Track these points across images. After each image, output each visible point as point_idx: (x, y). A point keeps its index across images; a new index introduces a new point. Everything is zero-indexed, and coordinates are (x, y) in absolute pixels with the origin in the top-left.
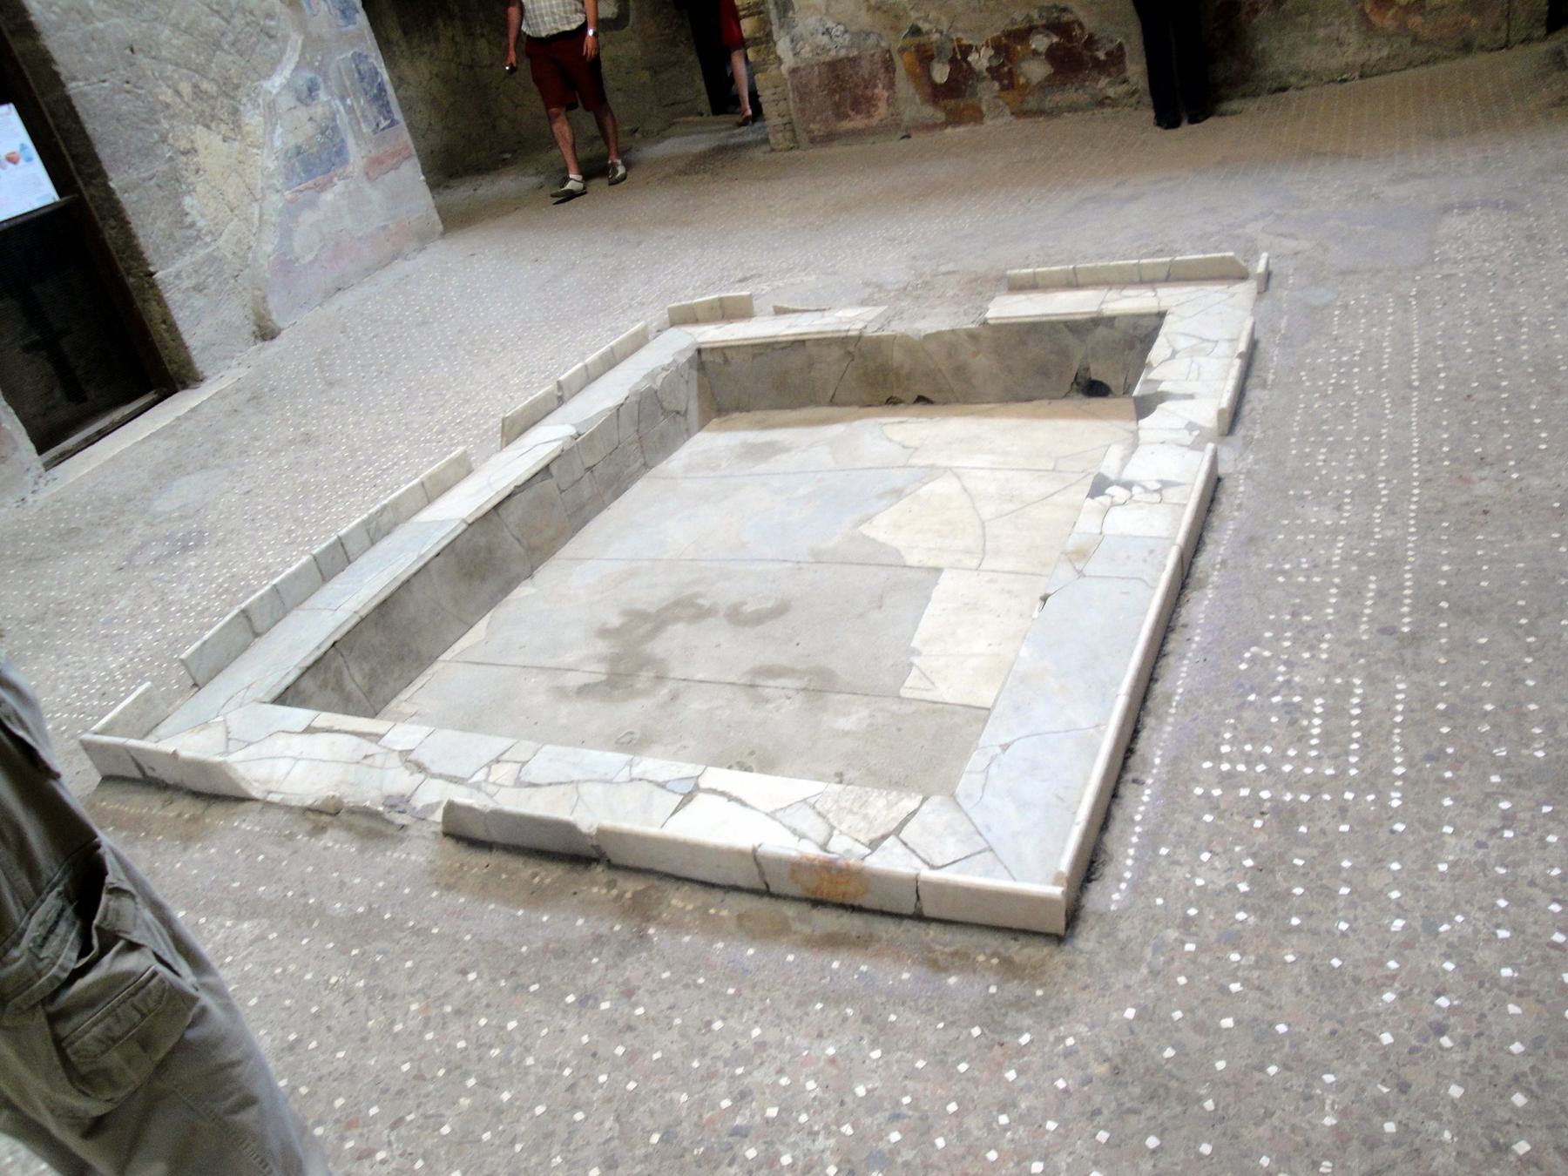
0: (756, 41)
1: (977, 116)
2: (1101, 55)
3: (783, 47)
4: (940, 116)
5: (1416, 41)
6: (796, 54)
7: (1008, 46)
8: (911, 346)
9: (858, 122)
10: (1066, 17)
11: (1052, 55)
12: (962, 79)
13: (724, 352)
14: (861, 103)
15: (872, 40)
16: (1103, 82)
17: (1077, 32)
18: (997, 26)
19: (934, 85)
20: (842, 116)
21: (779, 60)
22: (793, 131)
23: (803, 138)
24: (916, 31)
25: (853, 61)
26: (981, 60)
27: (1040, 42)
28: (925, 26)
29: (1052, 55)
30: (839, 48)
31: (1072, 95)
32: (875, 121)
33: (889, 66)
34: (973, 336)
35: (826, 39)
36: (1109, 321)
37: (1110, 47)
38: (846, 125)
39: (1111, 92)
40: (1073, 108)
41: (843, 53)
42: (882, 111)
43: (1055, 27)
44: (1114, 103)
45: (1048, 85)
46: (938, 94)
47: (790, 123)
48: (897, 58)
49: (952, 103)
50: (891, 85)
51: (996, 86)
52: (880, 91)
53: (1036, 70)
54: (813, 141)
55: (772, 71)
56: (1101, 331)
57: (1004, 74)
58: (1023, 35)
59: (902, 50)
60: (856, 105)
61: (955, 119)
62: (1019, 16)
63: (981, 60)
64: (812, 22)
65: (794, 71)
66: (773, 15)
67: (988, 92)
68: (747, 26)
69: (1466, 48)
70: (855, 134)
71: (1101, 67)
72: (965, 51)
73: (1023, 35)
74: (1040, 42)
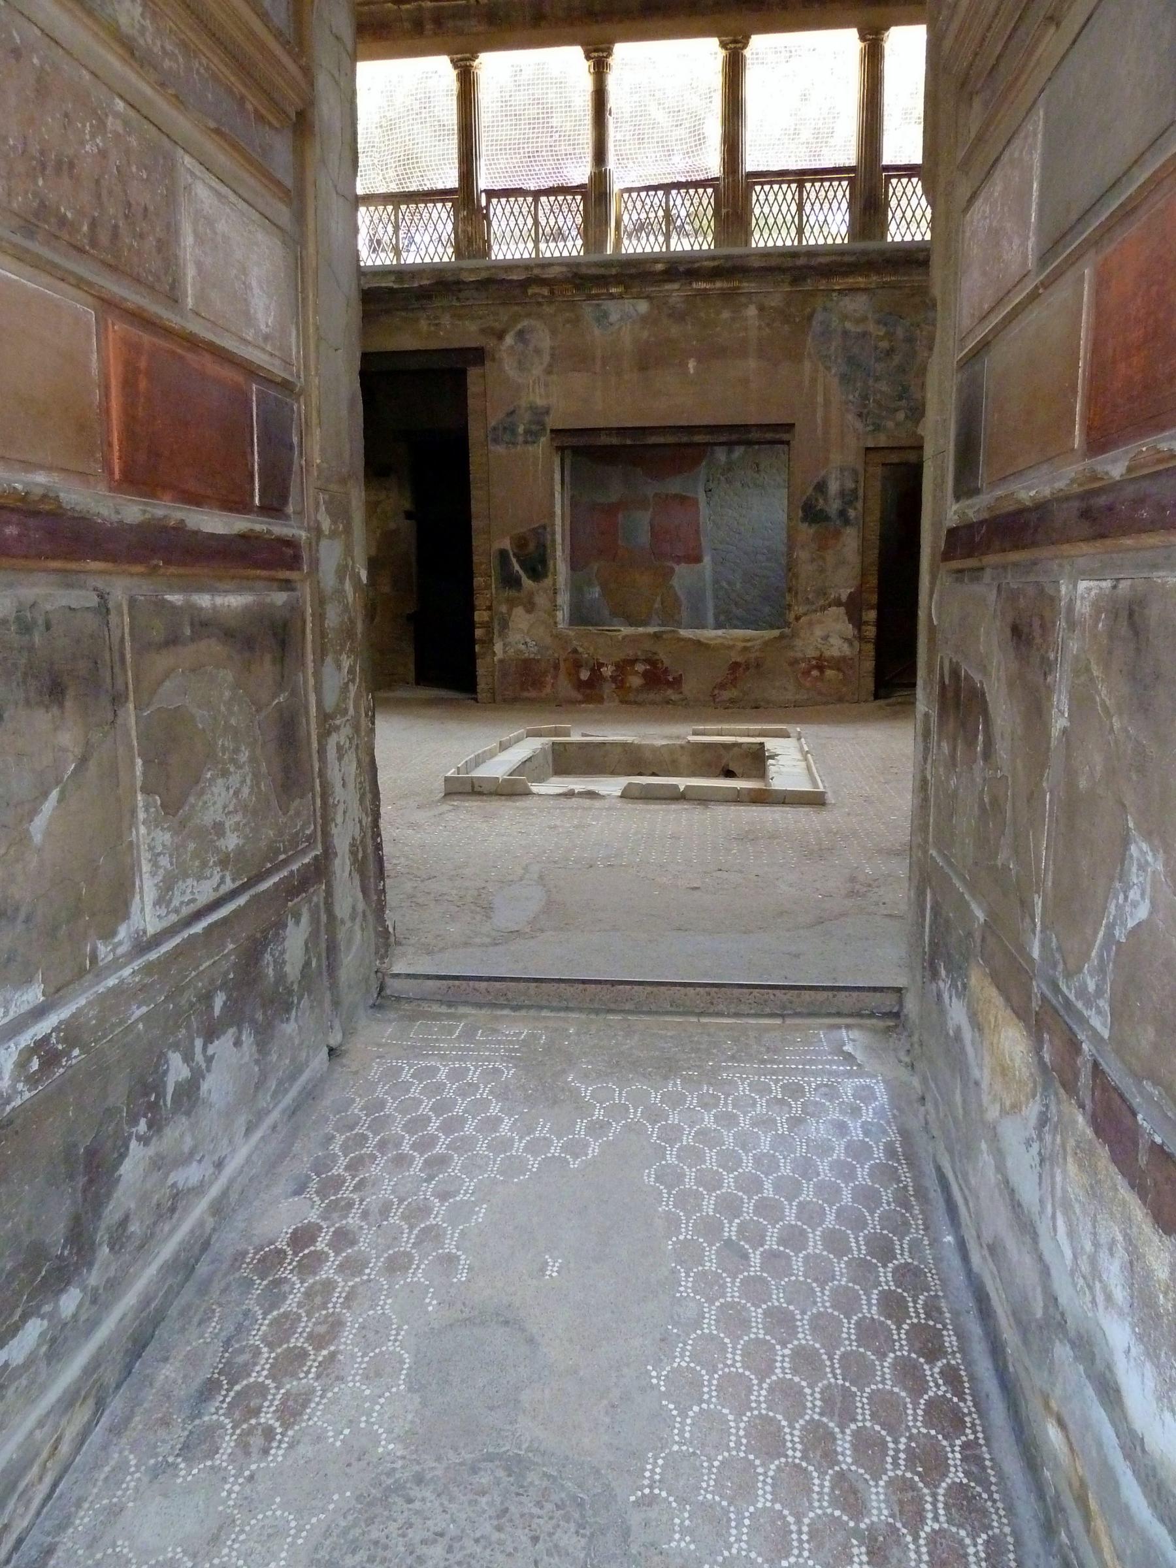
0: (483, 642)
1: (600, 700)
2: (671, 679)
3: (498, 647)
4: (580, 697)
5: (820, 693)
6: (505, 652)
7: (624, 666)
8: (655, 750)
9: (533, 694)
10: (656, 657)
11: (645, 674)
12: (596, 679)
13: (564, 744)
14: (537, 684)
15: (550, 652)
16: (670, 691)
17: (660, 665)
18: (619, 656)
19: (579, 679)
20: (523, 689)
21: (494, 654)
22: (493, 693)
23: (499, 698)
24: (575, 651)
25: (538, 661)
26: (608, 671)
27: (640, 667)
28: (580, 650)
29: (645, 674)
30: (531, 651)
31: (652, 696)
32: (543, 695)
33: (556, 667)
34: (682, 747)
35: (523, 647)
36: (739, 745)
37: (676, 675)
38: (526, 694)
39: (673, 698)
40: (653, 703)
41: (532, 656)
42: (548, 690)
43: (647, 661)
44: (674, 703)
45: (638, 691)
46: (580, 685)
47: (493, 689)
48: (562, 664)
49: (588, 691)
50: (555, 677)
51: (614, 686)
52: (549, 679)
53: (636, 681)
54: (504, 701)
55: (488, 659)
56: (736, 749)
57: (619, 681)
58: (633, 662)
59: (565, 660)
60: (534, 684)
61: (588, 699)
62: (631, 653)
63: (608, 671)
64: (518, 637)
65: (501, 661)
66: (496, 631)
67: (608, 689)
68: (479, 633)
69: (841, 700)
70: (532, 701)
71: (670, 684)
72: (602, 665)
73: (633, 662)
74: (640, 667)
